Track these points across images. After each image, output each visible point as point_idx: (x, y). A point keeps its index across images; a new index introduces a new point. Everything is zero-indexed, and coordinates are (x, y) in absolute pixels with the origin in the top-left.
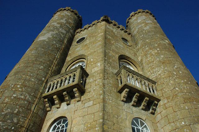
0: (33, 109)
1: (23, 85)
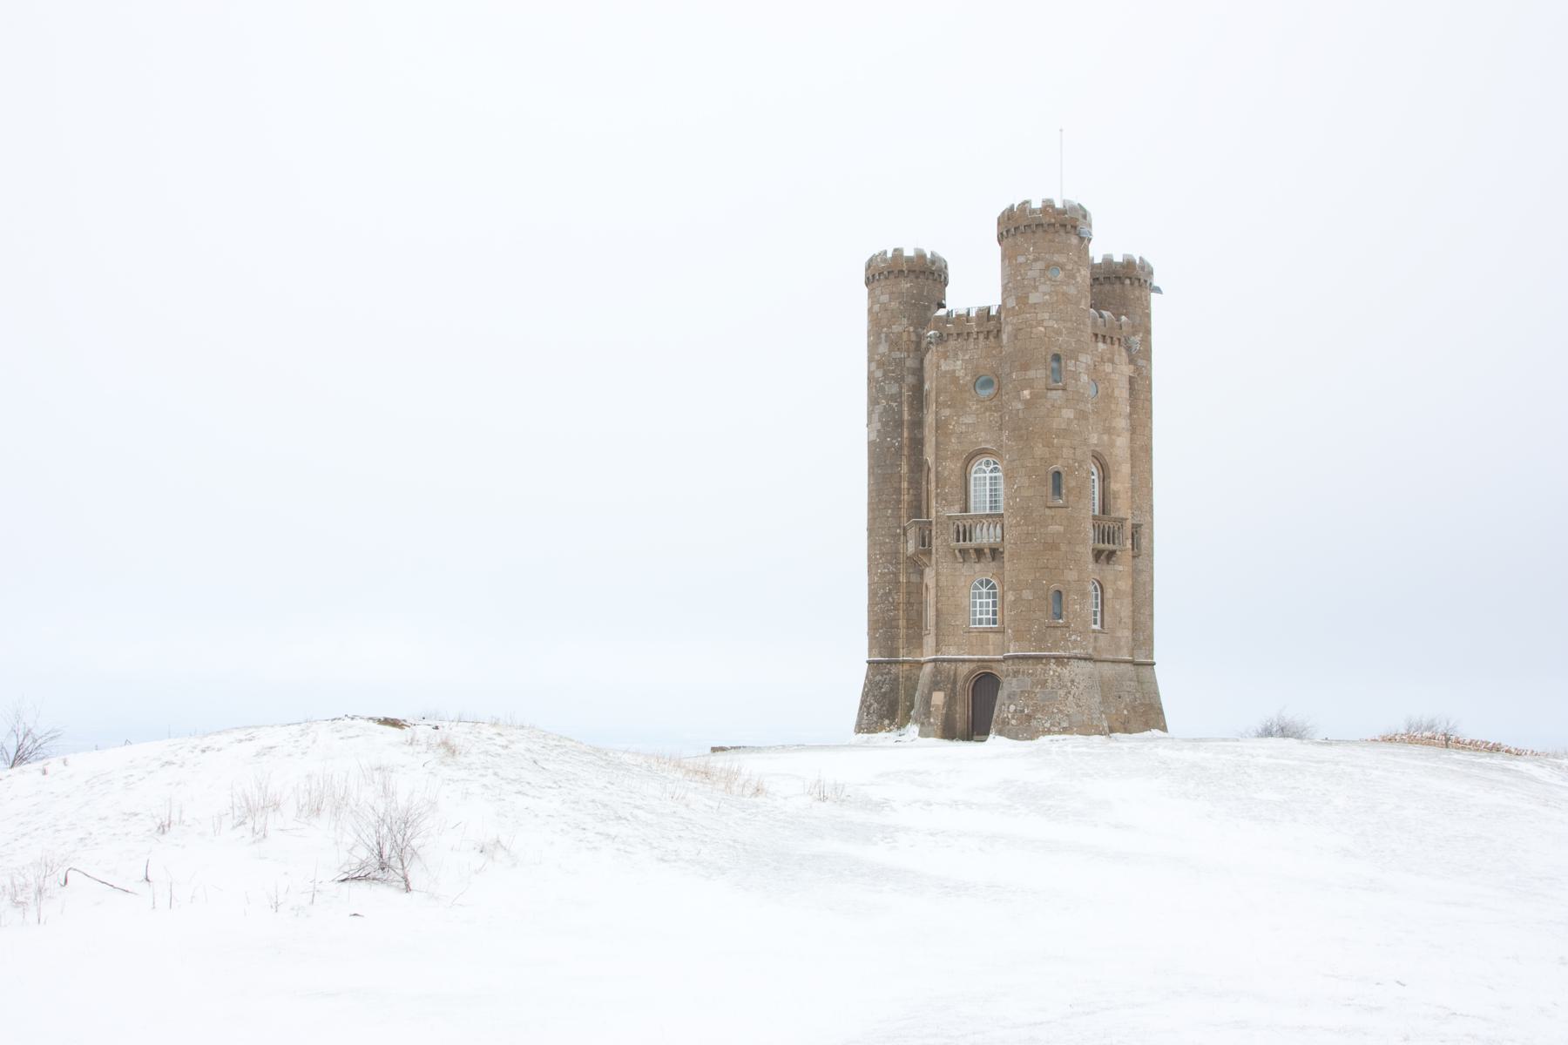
0: (901, 580)
1: (883, 554)
